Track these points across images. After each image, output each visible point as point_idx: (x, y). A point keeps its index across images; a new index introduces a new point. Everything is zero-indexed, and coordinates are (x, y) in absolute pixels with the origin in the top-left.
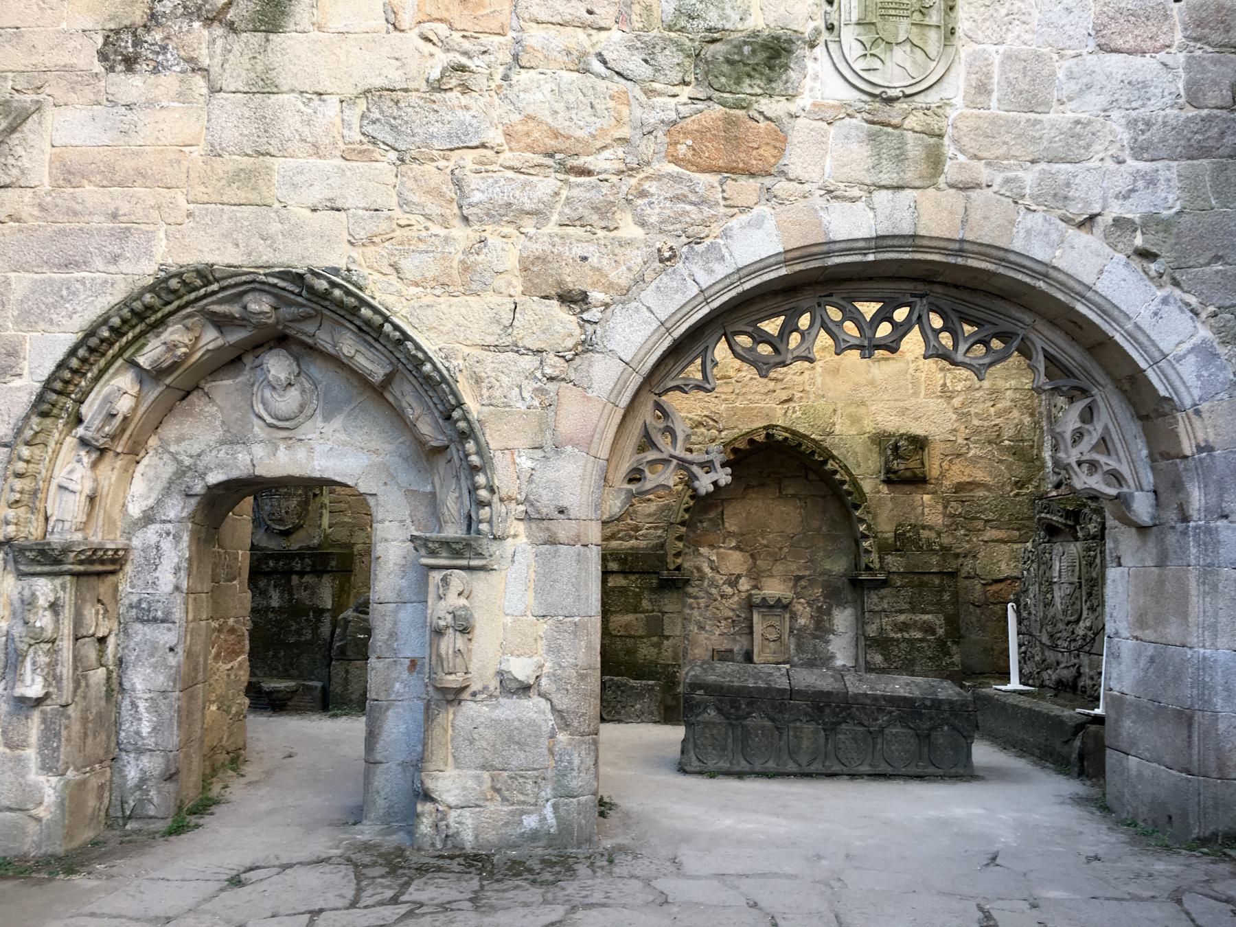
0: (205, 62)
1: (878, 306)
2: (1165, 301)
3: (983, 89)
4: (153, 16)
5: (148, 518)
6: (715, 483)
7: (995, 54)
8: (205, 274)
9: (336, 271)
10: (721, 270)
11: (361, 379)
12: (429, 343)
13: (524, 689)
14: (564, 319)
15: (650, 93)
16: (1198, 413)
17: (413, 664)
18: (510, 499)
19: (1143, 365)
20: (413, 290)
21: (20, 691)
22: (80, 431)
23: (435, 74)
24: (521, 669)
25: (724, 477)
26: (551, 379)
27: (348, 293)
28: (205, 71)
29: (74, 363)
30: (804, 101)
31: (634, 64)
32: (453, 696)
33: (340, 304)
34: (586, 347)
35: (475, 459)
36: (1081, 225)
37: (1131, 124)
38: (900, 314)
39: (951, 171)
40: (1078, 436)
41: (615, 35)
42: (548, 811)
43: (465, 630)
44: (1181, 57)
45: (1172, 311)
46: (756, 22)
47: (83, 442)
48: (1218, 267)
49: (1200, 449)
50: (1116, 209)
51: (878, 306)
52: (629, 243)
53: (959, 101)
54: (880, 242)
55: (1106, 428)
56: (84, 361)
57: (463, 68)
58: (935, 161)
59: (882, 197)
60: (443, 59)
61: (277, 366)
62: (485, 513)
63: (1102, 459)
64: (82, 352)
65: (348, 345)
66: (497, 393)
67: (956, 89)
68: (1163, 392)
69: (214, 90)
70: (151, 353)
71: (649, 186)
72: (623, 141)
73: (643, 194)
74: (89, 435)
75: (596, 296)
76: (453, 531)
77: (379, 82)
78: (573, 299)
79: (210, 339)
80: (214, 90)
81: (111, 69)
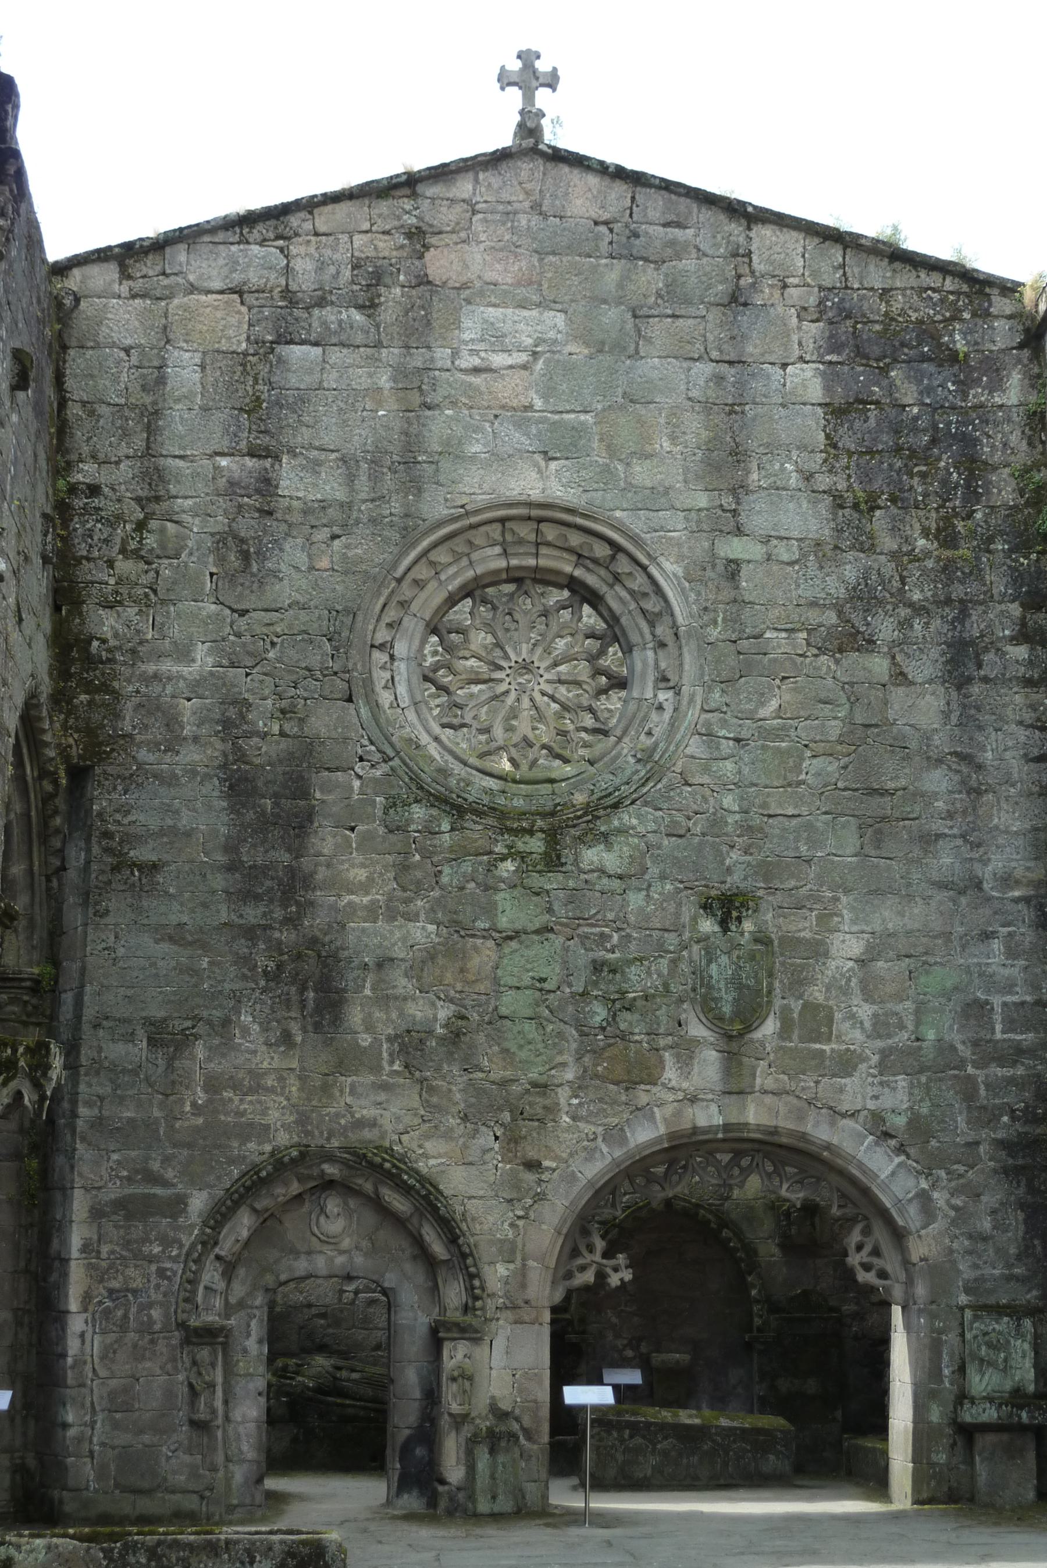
1: (731, 1155)
2: (900, 1165)
6: (622, 1280)
16: (920, 1237)
18: (494, 1295)
19: (889, 1205)
22: (217, 1250)
25: (627, 1275)
26: (519, 1217)
27: (394, 1166)
29: (224, 1209)
33: (389, 1172)
35: (472, 1270)
38: (745, 1162)
40: (859, 1248)
45: (902, 1174)
47: (218, 1258)
49: (921, 1260)
51: (731, 1155)
55: (877, 1240)
56: (228, 1208)
61: (333, 1204)
62: (479, 1304)
63: (875, 1261)
64: (229, 1203)
66: (486, 1227)
68: (900, 1222)
74: (223, 1253)
75: (546, 1163)
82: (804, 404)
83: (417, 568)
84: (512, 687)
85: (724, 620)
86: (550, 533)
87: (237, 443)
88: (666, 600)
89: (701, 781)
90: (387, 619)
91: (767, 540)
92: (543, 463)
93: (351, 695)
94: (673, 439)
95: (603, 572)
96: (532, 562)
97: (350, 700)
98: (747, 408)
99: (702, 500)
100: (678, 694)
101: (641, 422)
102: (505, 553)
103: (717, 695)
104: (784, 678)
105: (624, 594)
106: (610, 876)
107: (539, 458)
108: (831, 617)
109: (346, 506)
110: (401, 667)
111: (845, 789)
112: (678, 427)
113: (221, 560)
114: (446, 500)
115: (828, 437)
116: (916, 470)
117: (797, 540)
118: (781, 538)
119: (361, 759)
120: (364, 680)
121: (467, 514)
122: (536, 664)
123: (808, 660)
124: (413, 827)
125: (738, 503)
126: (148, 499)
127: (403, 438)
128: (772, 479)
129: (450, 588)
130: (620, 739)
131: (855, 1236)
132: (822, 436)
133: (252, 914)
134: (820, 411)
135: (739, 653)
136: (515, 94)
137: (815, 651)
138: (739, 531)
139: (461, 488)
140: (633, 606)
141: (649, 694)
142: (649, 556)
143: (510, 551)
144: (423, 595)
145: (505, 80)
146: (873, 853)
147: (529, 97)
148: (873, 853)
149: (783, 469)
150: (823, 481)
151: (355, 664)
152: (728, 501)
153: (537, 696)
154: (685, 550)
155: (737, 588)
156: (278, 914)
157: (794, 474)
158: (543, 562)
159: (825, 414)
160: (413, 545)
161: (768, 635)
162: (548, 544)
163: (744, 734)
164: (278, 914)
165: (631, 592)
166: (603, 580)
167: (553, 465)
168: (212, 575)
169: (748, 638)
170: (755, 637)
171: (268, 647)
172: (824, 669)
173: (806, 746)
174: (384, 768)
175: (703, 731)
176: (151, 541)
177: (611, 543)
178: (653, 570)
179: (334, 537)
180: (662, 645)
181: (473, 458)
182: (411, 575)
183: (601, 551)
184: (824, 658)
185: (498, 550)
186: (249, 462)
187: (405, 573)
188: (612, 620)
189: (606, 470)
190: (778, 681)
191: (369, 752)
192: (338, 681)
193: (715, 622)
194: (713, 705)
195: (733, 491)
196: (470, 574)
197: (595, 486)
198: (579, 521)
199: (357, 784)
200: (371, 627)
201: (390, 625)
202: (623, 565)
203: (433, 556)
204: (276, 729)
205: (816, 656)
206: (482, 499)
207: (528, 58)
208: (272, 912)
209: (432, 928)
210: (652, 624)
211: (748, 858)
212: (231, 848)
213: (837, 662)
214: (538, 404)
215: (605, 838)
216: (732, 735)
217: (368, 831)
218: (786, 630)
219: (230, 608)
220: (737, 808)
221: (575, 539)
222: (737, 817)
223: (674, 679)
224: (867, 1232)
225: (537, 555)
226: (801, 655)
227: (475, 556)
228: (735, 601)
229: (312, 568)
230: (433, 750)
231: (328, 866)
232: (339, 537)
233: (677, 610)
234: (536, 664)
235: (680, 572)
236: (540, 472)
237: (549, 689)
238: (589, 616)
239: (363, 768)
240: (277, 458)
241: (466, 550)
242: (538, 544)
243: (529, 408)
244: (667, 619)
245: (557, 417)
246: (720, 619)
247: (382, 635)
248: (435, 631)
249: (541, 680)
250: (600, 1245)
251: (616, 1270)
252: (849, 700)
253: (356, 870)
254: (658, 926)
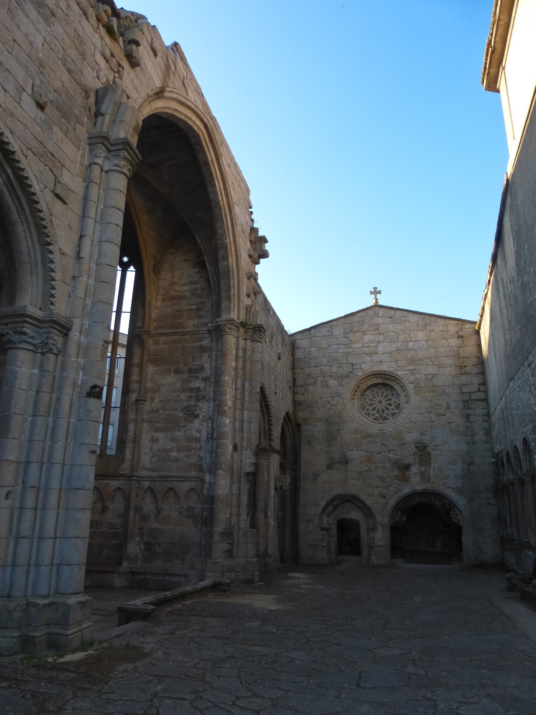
0: (339, 468)
2: (460, 498)
3: (434, 470)
4: (332, 462)
5: (332, 524)
7: (436, 465)
8: (341, 495)
9: (356, 494)
10: (403, 494)
11: (358, 507)
12: (367, 503)
13: (381, 546)
14: (384, 500)
15: (393, 471)
17: (366, 543)
20: (365, 497)
21: (323, 545)
23: (367, 469)
24: (381, 544)
28: (339, 469)
30: (412, 472)
31: (391, 468)
32: (373, 547)
34: (386, 504)
36: (448, 488)
37: (454, 475)
39: (431, 481)
40: (453, 514)
41: (388, 464)
42: (385, 561)
43: (374, 539)
44: (461, 466)
46: (406, 462)
48: (467, 493)
50: (453, 486)
52: (391, 491)
53: (432, 472)
54: (422, 490)
57: (370, 469)
58: (429, 480)
59: (423, 484)
60: (367, 467)
61: (348, 504)
63: (456, 517)
65: (357, 503)
67: (431, 470)
68: (460, 509)
69: (340, 472)
70: (334, 504)
71: (393, 483)
72: (390, 478)
73: (393, 484)
76: (371, 526)
77: (360, 471)
78: (385, 497)
79: (340, 501)
80: (340, 472)
81: (328, 469)
107: (380, 362)
131: (452, 512)
136: (373, 296)
145: (371, 293)
147: (376, 296)
179: (343, 380)
207: (375, 288)
224: (454, 511)
250: (400, 513)
251: (403, 518)
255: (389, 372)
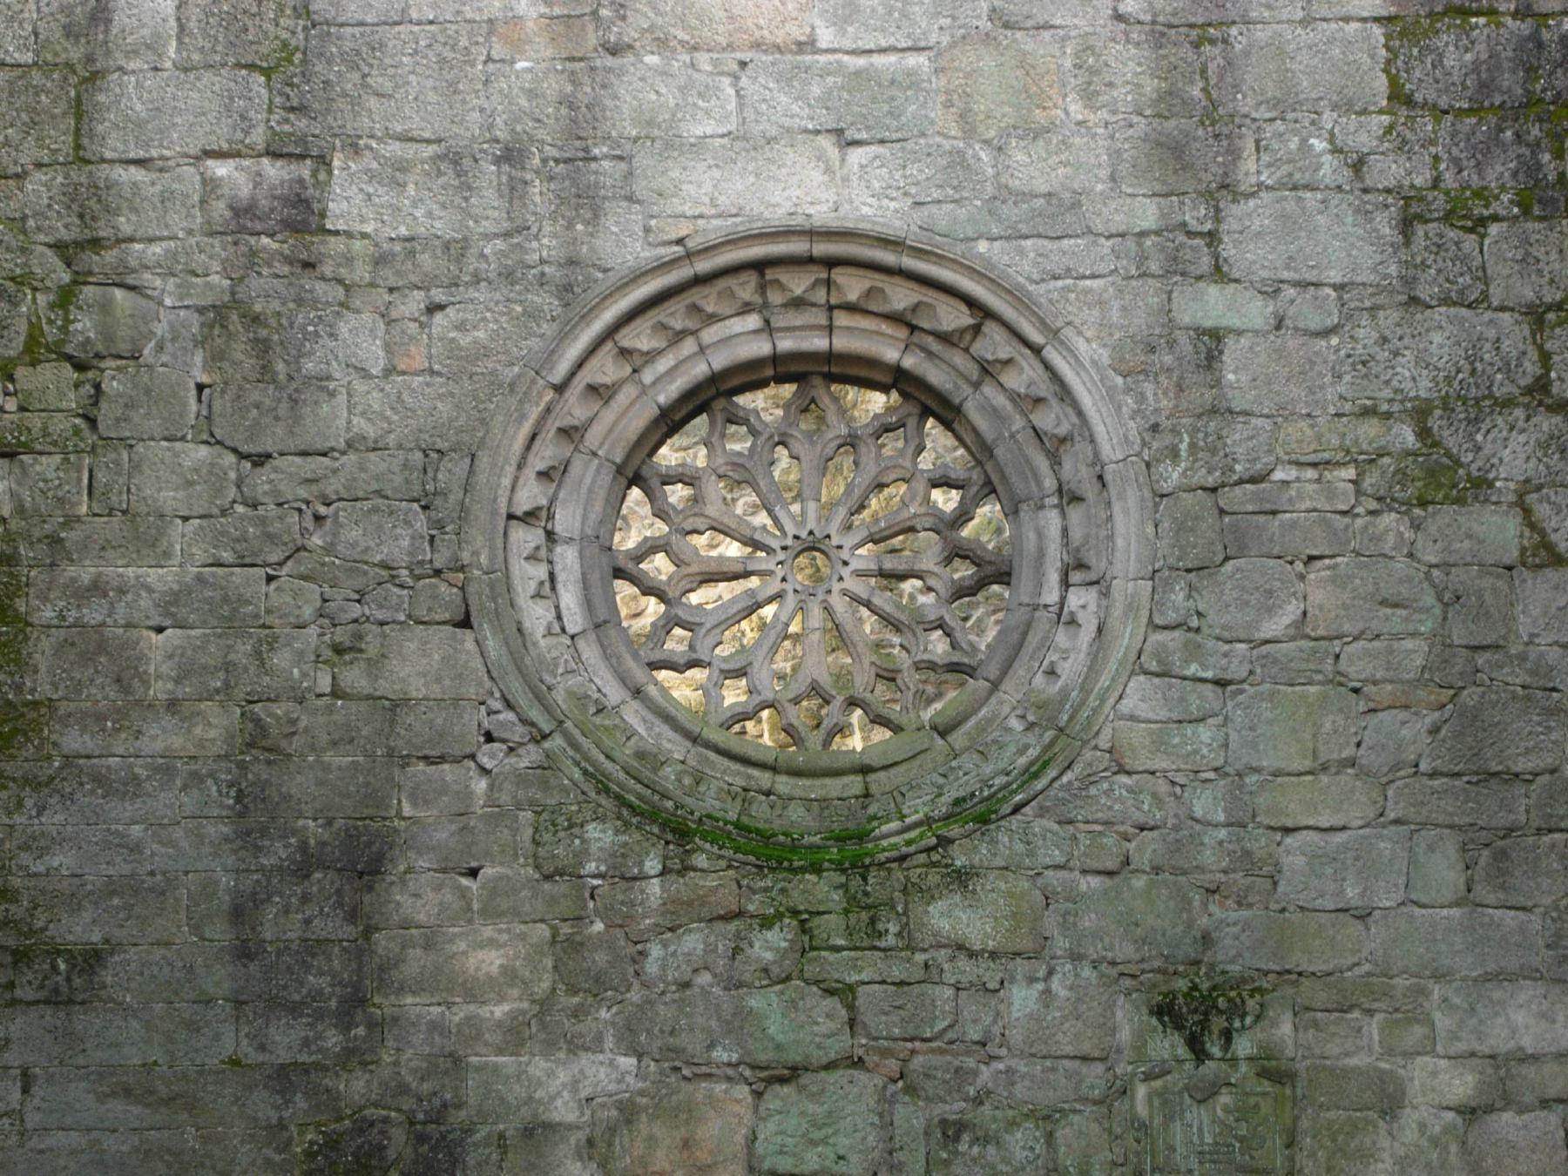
82: (1347, 19)
83: (594, 362)
84: (789, 587)
85: (1193, 446)
86: (852, 286)
87: (247, 133)
88: (1080, 413)
89: (1150, 765)
90: (538, 463)
91: (1271, 291)
92: (833, 153)
93: (468, 614)
94: (1089, 97)
95: (959, 359)
96: (819, 343)
97: (465, 623)
98: (1234, 31)
99: (1147, 214)
100: (1106, 594)
101: (1024, 63)
102: (768, 328)
103: (1179, 596)
104: (1311, 558)
105: (1000, 400)
106: (972, 955)
107: (826, 143)
108: (1407, 436)
109: (456, 249)
110: (568, 558)
111: (1434, 774)
112: (1098, 72)
113: (216, 358)
114: (647, 230)
115: (1394, 82)
116: (739, 511)
117: (1335, 287)
118: (1303, 285)
119: (489, 738)
120: (492, 586)
121: (690, 255)
122: (835, 541)
123: (1359, 522)
124: (591, 867)
125: (1218, 220)
126: (79, 245)
127: (564, 111)
128: (1286, 169)
129: (662, 399)
130: (995, 685)
132: (1381, 83)
133: (286, 1040)
134: (1378, 31)
135: (1222, 512)
137: (1373, 505)
138: (1219, 273)
139: (675, 205)
140: (1018, 423)
141: (1051, 596)
142: (1043, 325)
143: (778, 321)
144: (608, 416)
146: (1491, 899)
148: (1491, 899)
149: (1304, 146)
150: (1389, 170)
151: (476, 553)
152: (1195, 215)
153: (839, 604)
154: (1115, 315)
155: (1217, 383)
156: (333, 1040)
157: (1327, 158)
158: (841, 343)
159: (1388, 37)
160: (586, 318)
161: (1278, 475)
162: (851, 308)
163: (1237, 670)
164: (333, 1040)
165: (1014, 397)
166: (962, 375)
167: (857, 156)
168: (200, 388)
169: (1240, 482)
170: (1253, 480)
171: (309, 523)
172: (1391, 540)
173: (1356, 691)
174: (530, 756)
175: (1153, 666)
176: (84, 325)
177: (971, 303)
178: (1051, 354)
179: (433, 308)
180: (1076, 499)
181: (698, 147)
182: (586, 376)
183: (952, 317)
184: (1389, 519)
185: (753, 321)
186: (273, 171)
187: (572, 374)
188: (981, 451)
189: (958, 161)
190: (1299, 566)
191: (502, 724)
192: (443, 588)
193: (1175, 454)
194: (1172, 617)
195: (1208, 196)
196: (700, 370)
197: (936, 194)
198: (909, 262)
199: (481, 785)
200: (506, 482)
201: (544, 475)
202: (995, 343)
203: (627, 338)
204: (325, 683)
205: (1372, 513)
206: (716, 229)
208: (320, 1037)
209: (628, 1062)
210: (1055, 461)
211: (1245, 913)
212: (241, 912)
213: (1416, 526)
214: (825, 37)
215: (962, 879)
216: (1209, 674)
217: (501, 877)
218: (1314, 465)
219: (235, 450)
220: (1221, 817)
221: (901, 296)
222: (1223, 833)
223: (1098, 565)
225: (830, 329)
226: (1344, 513)
227: (710, 334)
228: (1214, 411)
229: (390, 371)
230: (633, 715)
231: (428, 946)
232: (441, 307)
233: (1100, 430)
234: (835, 541)
235: (1104, 356)
236: (828, 170)
237: (859, 587)
238: (938, 441)
239: (492, 756)
240: (323, 161)
241: (691, 324)
242: (831, 308)
243: (807, 45)
244: (1082, 448)
245: (861, 62)
246: (1184, 447)
247: (530, 495)
248: (636, 480)
249: (846, 572)
252: (1440, 599)
253: (481, 954)
254: (1069, 1050)
255: (919, 253)
